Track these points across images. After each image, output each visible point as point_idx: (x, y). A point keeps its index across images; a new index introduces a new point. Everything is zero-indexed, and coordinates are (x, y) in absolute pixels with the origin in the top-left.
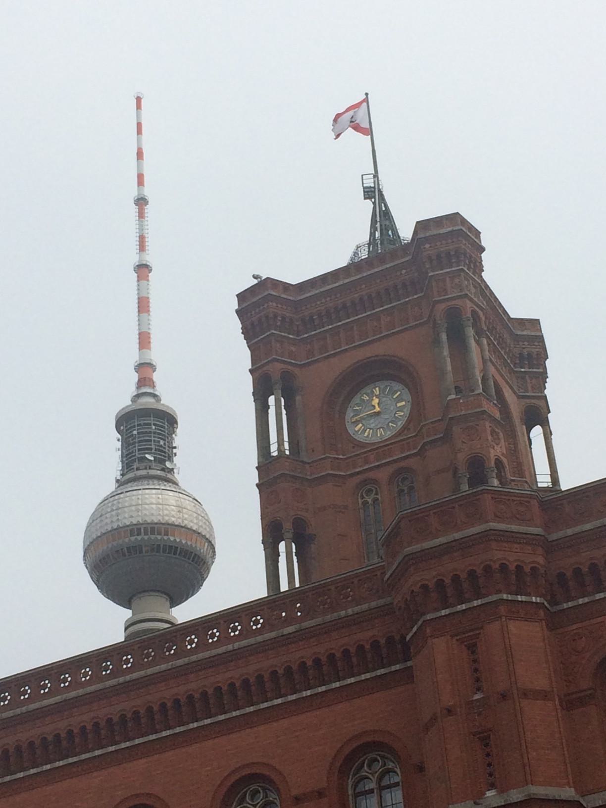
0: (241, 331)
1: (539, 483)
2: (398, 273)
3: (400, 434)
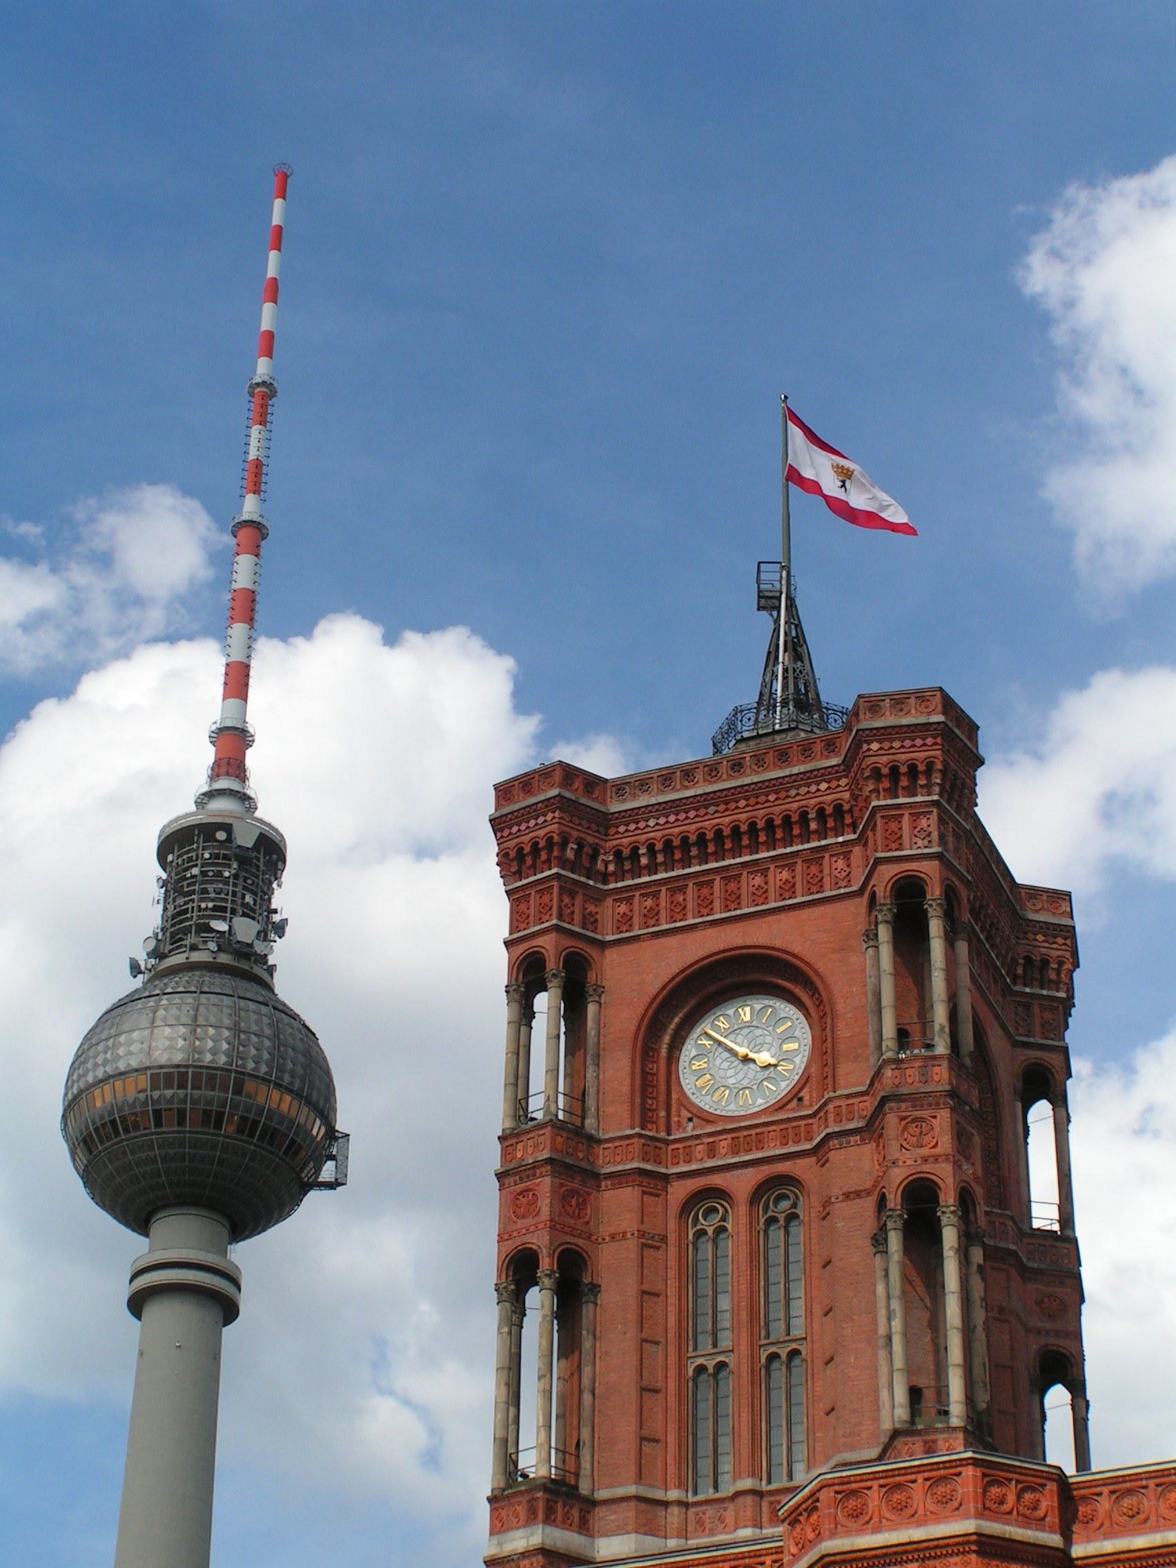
0: (496, 859)
1: (1034, 1220)
2: (813, 788)
3: (781, 1108)
